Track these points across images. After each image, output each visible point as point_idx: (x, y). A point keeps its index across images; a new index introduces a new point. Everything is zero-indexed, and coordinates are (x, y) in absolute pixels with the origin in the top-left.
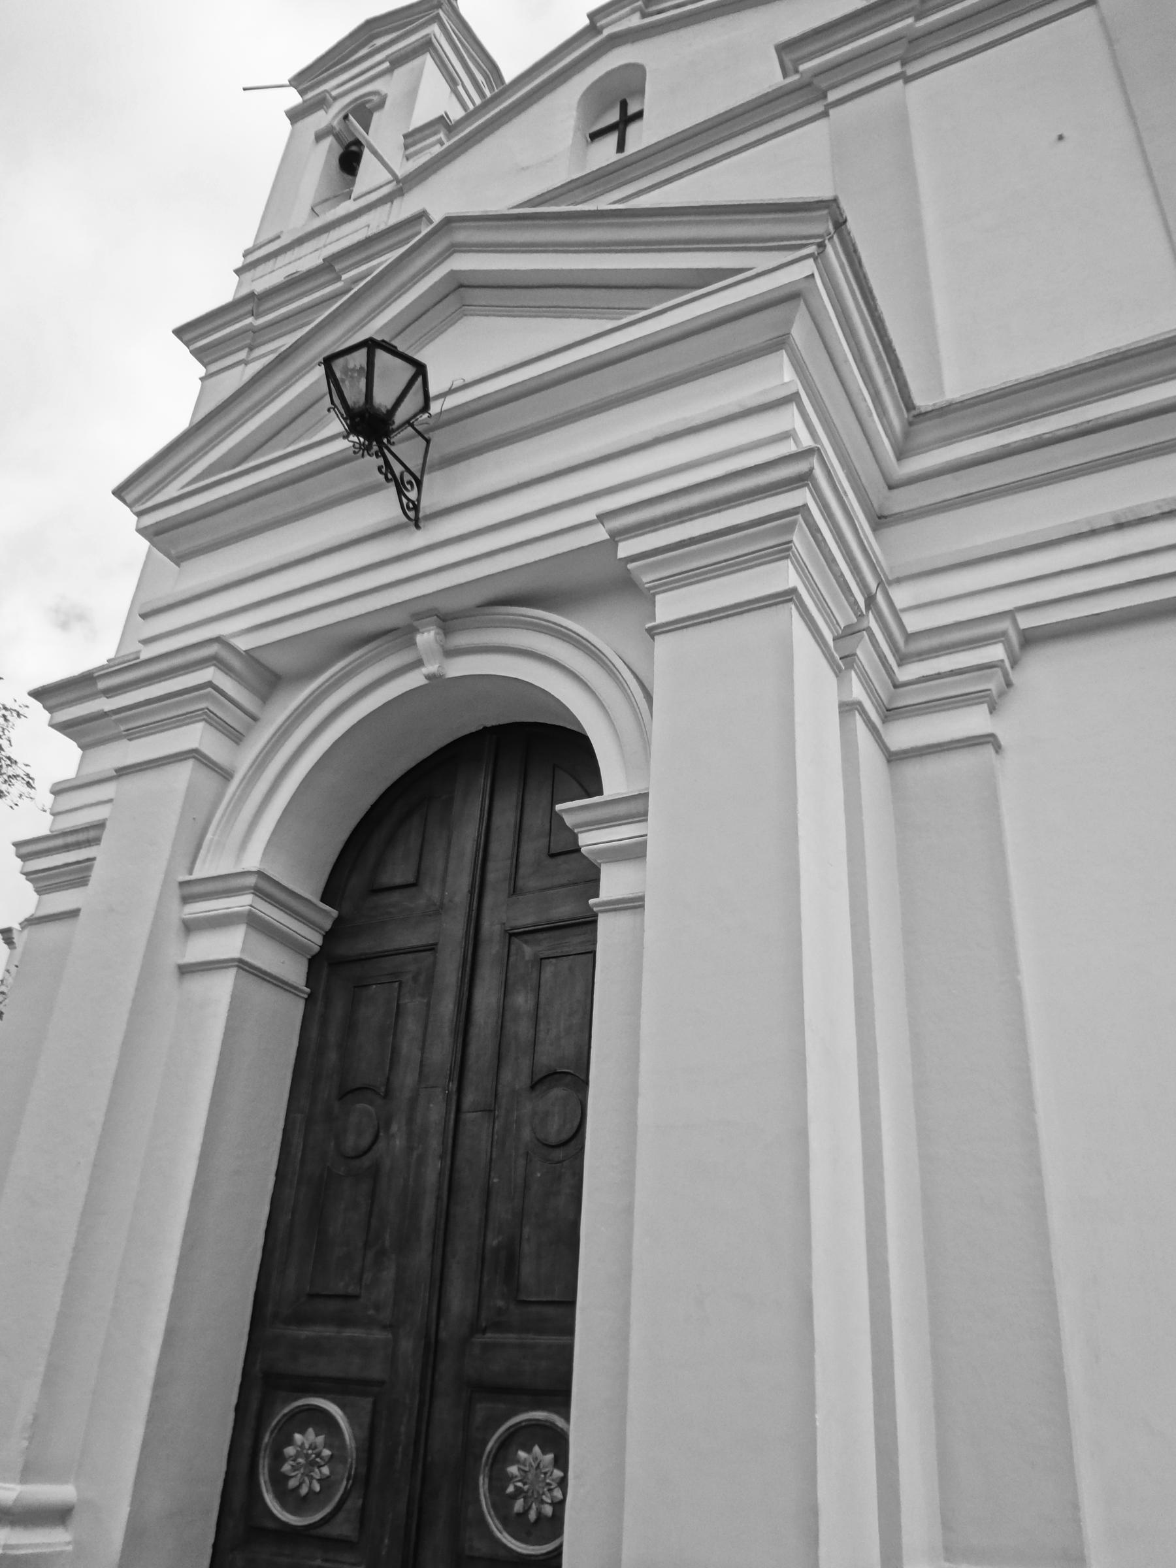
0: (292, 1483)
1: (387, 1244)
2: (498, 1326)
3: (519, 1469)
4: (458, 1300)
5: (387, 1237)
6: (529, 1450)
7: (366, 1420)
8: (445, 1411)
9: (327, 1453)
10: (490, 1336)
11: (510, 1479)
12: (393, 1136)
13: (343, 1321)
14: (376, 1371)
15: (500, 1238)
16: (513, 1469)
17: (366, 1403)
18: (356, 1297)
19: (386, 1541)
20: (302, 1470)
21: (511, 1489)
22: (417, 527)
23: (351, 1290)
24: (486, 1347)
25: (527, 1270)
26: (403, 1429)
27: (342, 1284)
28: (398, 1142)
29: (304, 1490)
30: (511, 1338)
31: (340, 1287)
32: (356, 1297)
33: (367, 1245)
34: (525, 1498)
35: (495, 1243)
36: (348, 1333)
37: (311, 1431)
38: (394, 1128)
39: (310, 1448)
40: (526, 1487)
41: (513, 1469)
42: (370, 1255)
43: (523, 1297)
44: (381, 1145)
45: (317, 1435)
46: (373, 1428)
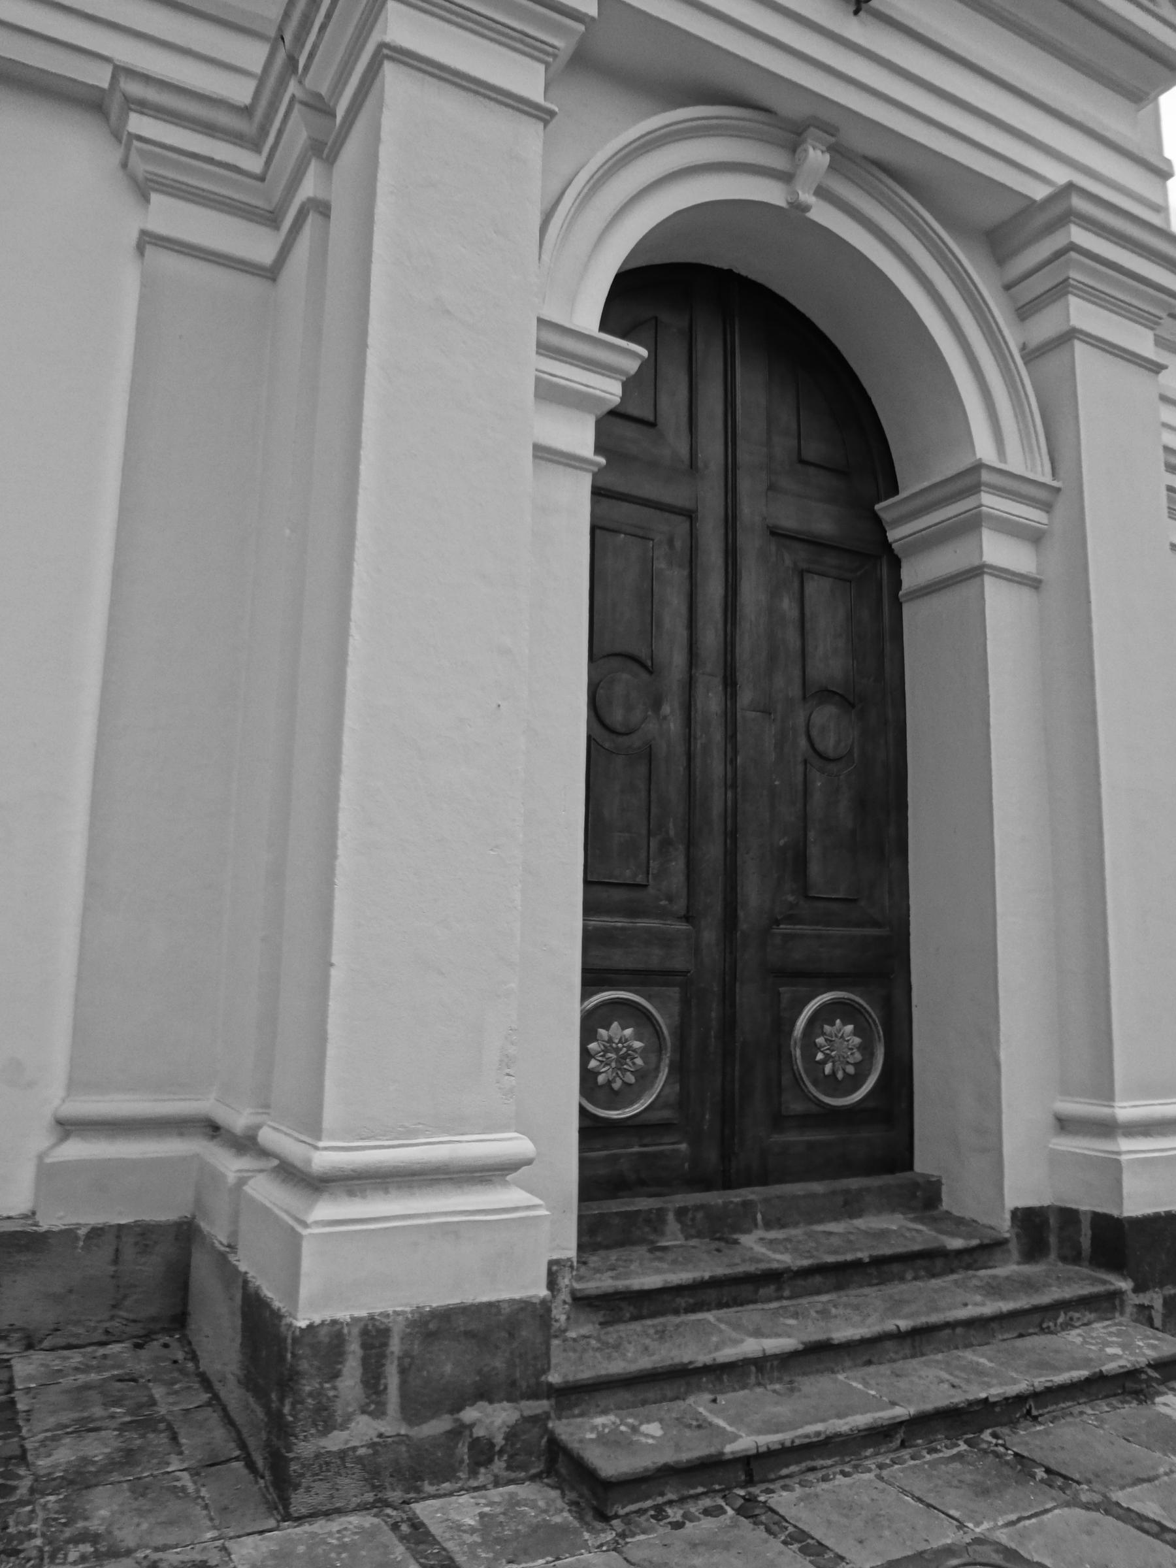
0: (601, 1079)
1: (672, 833)
2: (791, 919)
3: (826, 1040)
4: (754, 893)
5: (671, 825)
6: (833, 1024)
7: (676, 1009)
8: (748, 996)
9: (637, 1044)
10: (785, 928)
11: (818, 1048)
12: (665, 718)
13: (633, 912)
14: (679, 961)
15: (786, 839)
16: (820, 1040)
17: (674, 992)
18: (646, 886)
19: (707, 1117)
20: (613, 1065)
21: (820, 1056)
22: (856, 12)
23: (640, 879)
24: (788, 938)
25: (815, 869)
26: (713, 1015)
27: (628, 873)
28: (672, 725)
29: (617, 1085)
30: (806, 929)
31: (627, 875)
32: (646, 886)
33: (649, 834)
34: (834, 1062)
35: (782, 843)
36: (642, 923)
37: (615, 1025)
38: (666, 709)
39: (620, 1041)
40: (833, 1053)
41: (820, 1040)
42: (654, 844)
43: (813, 894)
44: (652, 726)
45: (623, 1029)
46: (684, 1015)
